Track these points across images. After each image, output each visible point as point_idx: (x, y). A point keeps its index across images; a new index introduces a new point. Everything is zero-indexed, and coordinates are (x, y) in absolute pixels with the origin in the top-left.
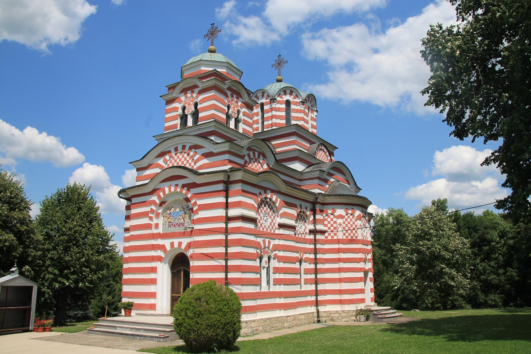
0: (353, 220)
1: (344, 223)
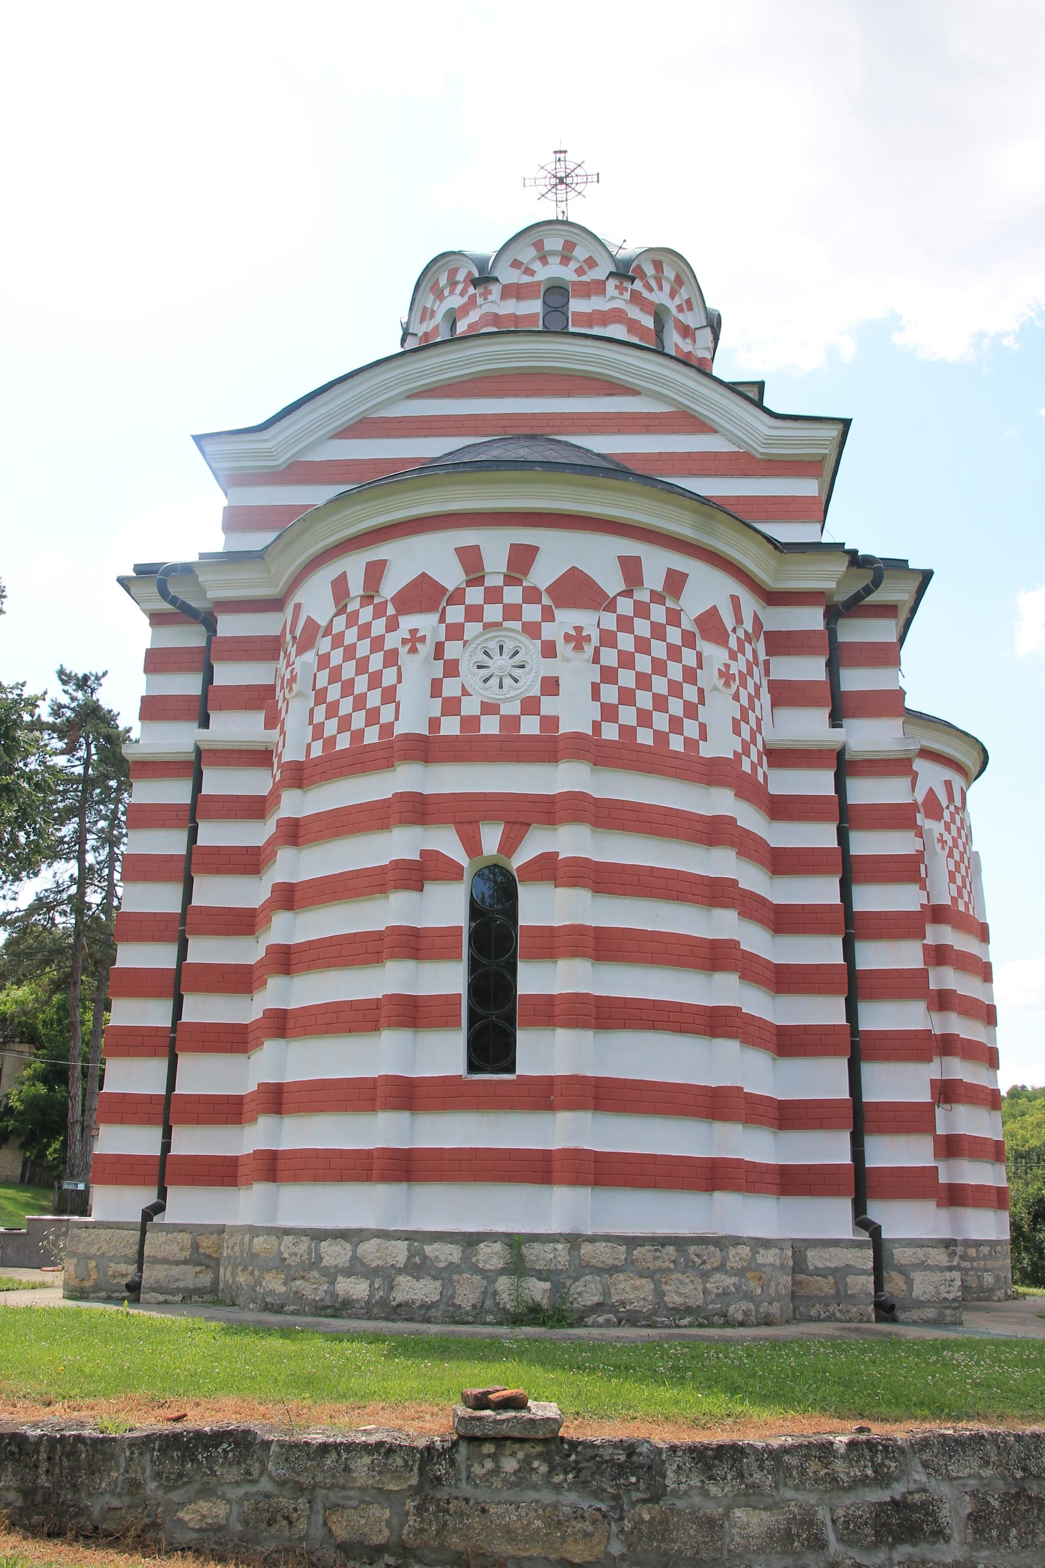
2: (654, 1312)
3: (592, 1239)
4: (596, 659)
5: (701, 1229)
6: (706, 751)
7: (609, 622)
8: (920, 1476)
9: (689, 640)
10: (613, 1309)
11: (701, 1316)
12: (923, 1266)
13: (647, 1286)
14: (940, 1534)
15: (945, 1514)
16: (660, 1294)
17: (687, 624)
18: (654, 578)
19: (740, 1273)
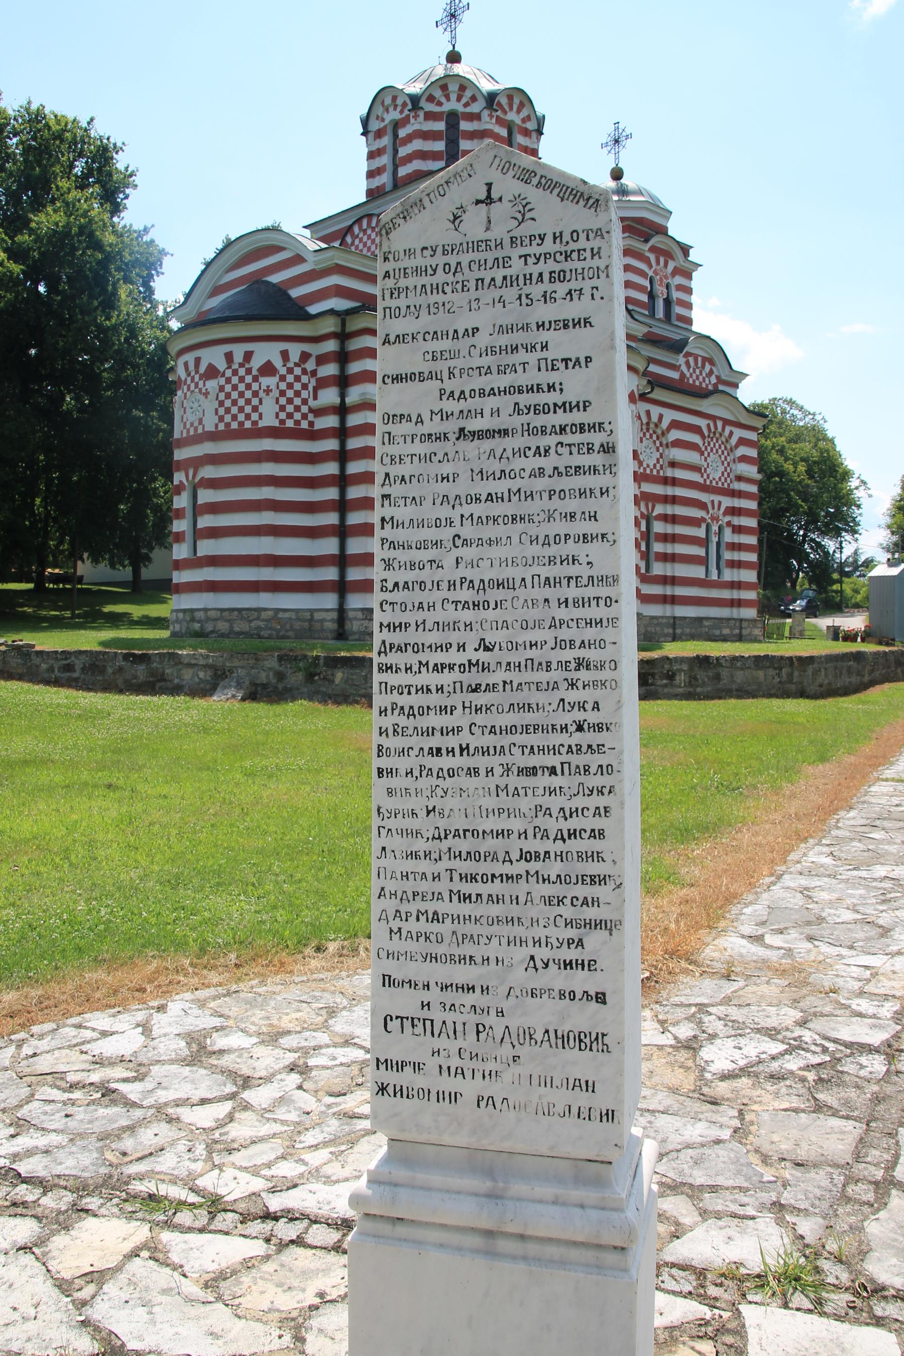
2: (229, 633)
4: (217, 398)
5: (254, 605)
6: (261, 424)
7: (222, 381)
8: (73, 658)
9: (255, 379)
10: (217, 632)
11: (248, 635)
12: (355, 619)
13: (227, 625)
14: (75, 671)
15: (76, 667)
16: (231, 627)
17: (255, 372)
18: (238, 358)
19: (268, 621)
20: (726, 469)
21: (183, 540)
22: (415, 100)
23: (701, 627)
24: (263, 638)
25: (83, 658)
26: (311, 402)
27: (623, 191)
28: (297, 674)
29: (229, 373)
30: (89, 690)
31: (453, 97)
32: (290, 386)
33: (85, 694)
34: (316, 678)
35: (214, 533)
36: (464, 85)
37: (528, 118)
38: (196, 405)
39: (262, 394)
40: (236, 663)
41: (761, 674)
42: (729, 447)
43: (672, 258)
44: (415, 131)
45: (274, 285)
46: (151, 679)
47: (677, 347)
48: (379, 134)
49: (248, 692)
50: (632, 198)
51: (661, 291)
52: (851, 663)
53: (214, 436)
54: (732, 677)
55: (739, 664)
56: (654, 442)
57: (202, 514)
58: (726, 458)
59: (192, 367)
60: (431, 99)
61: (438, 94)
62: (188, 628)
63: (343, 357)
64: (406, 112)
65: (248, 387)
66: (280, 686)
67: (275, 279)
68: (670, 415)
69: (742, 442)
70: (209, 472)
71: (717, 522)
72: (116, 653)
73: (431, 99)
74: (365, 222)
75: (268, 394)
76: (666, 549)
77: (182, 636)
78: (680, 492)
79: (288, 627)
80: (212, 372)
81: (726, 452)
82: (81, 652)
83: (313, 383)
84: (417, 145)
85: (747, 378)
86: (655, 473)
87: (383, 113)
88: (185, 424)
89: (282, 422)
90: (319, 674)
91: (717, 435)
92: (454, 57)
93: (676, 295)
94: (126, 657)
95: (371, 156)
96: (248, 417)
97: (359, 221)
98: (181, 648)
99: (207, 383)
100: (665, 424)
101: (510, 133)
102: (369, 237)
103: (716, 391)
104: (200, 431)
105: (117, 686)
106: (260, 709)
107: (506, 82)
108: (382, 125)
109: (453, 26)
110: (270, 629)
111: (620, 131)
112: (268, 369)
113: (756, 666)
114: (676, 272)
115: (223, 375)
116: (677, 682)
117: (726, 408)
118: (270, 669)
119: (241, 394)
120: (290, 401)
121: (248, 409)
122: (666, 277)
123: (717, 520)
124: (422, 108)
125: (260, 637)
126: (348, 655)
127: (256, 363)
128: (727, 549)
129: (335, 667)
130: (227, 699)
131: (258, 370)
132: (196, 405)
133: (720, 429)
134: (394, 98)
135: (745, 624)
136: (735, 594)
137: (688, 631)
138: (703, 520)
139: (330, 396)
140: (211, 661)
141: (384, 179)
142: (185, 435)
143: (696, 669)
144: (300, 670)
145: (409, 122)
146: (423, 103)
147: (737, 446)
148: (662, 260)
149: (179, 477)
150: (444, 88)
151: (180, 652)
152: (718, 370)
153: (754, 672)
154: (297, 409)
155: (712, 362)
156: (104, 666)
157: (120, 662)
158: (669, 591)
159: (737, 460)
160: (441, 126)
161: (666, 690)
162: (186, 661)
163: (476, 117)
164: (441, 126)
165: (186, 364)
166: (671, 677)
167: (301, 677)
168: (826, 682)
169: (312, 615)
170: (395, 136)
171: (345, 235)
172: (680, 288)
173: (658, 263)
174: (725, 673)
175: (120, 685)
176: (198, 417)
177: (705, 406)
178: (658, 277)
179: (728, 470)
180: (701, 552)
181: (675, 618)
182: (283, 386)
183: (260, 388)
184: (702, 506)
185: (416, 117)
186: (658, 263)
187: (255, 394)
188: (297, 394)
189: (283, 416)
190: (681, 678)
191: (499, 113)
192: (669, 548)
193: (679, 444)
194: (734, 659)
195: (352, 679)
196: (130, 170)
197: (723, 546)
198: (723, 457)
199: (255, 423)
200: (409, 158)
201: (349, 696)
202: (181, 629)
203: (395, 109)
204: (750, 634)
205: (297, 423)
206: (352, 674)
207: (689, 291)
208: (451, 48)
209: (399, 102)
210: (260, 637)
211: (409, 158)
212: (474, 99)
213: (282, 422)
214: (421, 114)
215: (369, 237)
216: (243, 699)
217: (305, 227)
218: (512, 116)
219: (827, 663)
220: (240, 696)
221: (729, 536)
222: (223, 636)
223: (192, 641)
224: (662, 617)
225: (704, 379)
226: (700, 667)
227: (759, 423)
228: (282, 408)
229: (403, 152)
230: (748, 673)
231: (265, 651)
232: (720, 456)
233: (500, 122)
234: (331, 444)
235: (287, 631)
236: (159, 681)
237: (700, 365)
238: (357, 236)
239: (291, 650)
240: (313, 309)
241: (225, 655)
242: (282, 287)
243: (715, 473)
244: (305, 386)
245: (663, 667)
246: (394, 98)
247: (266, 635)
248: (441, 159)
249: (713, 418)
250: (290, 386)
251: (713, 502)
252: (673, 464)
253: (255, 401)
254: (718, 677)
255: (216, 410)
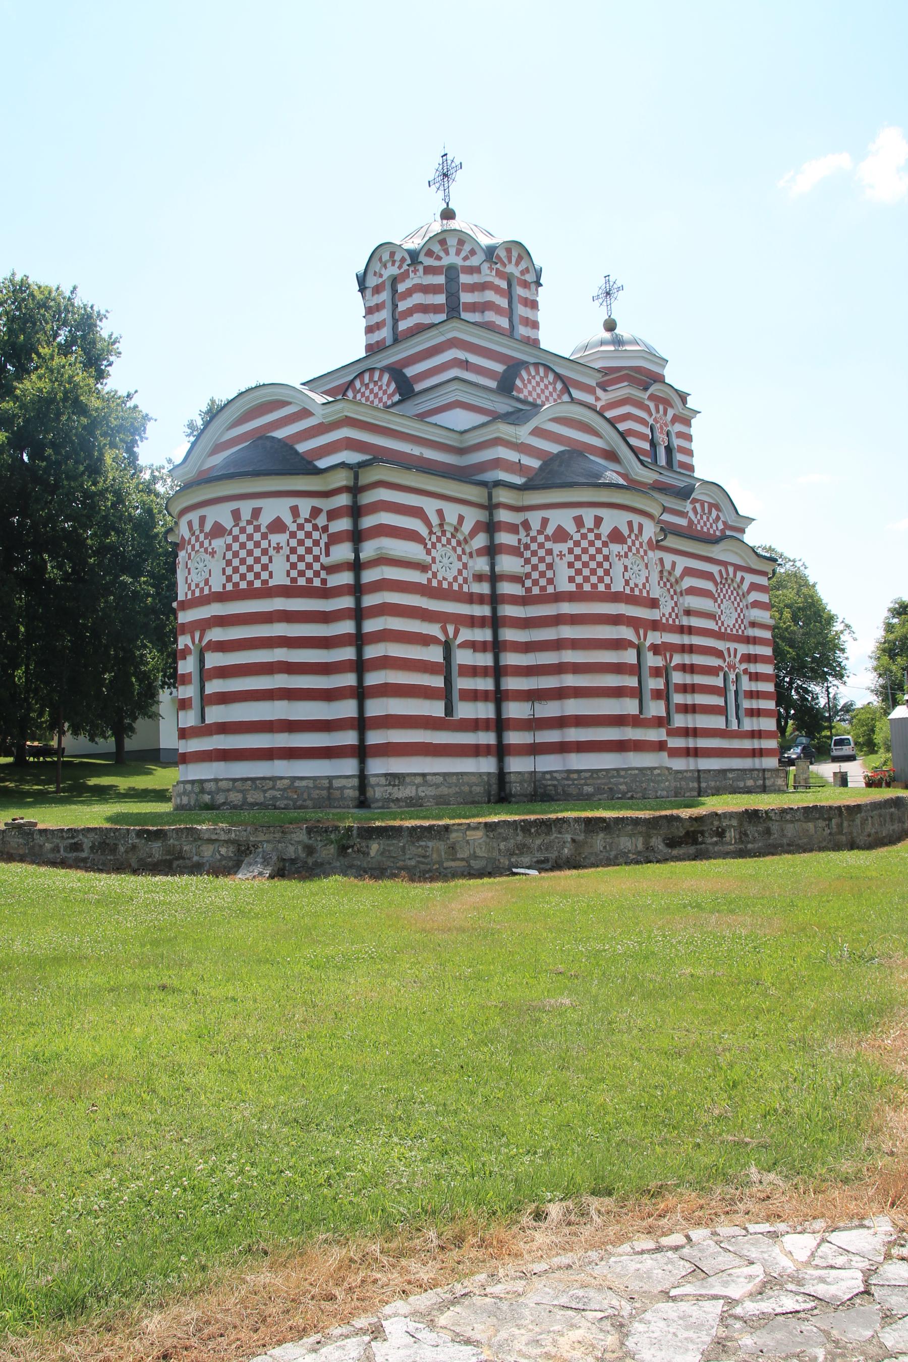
0: (598, 544)
1: (571, 551)
2: (242, 805)
3: (222, 780)
4: (224, 558)
5: (268, 774)
6: (272, 583)
7: (229, 539)
8: (81, 837)
9: (264, 536)
10: (229, 804)
11: (262, 806)
12: (378, 785)
13: (240, 796)
14: (83, 850)
15: (84, 846)
16: (245, 798)
18: (246, 515)
19: (284, 790)
20: (739, 615)
21: (190, 707)
22: (414, 255)
23: (725, 779)
24: (279, 808)
25: (91, 835)
26: (323, 559)
27: (618, 342)
28: (328, 847)
29: (236, 531)
30: (100, 871)
31: (452, 251)
32: (301, 543)
33: (97, 875)
34: (350, 850)
35: (224, 698)
36: (462, 239)
37: (527, 270)
38: (201, 565)
39: (271, 552)
40: (262, 837)
41: (811, 826)
42: (741, 593)
43: (672, 407)
44: (414, 285)
45: (280, 440)
46: (168, 857)
47: (685, 493)
48: (377, 290)
49: (276, 869)
50: (628, 348)
51: (661, 439)
52: (893, 810)
53: (221, 597)
54: (782, 830)
55: (788, 817)
56: (668, 590)
57: (210, 678)
58: (739, 605)
59: (196, 526)
60: (430, 253)
61: (437, 248)
62: (197, 800)
63: (356, 512)
64: (405, 267)
65: (257, 545)
66: (310, 861)
67: (280, 434)
68: (683, 563)
69: (754, 587)
70: (216, 634)
71: (734, 671)
72: (128, 830)
73: (430, 253)
74: (367, 377)
75: (278, 552)
76: (686, 699)
77: (190, 809)
78: (697, 640)
79: (305, 796)
80: (218, 531)
81: (738, 598)
82: (89, 830)
83: (325, 538)
84: (418, 298)
85: (754, 522)
86: (671, 622)
87: (381, 269)
88: (190, 586)
89: (294, 580)
90: (352, 847)
91: (729, 581)
92: (448, 214)
93: (677, 442)
94: (139, 834)
95: (370, 311)
96: (257, 576)
97: (360, 375)
98: (200, 822)
99: (213, 542)
100: (678, 572)
101: (510, 285)
102: (372, 391)
103: (724, 538)
104: (206, 591)
105: (130, 865)
106: (291, 888)
107: (501, 236)
108: (381, 280)
109: (446, 185)
110: (287, 798)
111: (611, 284)
112: (278, 526)
113: (805, 818)
114: (676, 419)
115: (230, 533)
116: (727, 839)
117: (736, 553)
118: (299, 842)
119: (250, 553)
120: (301, 558)
121: (257, 568)
122: (666, 426)
123: (734, 668)
124: (421, 263)
125: (276, 808)
126: (383, 825)
127: (265, 520)
128: (745, 697)
129: (370, 838)
130: (254, 877)
131: (268, 527)
132: (201, 565)
133: (731, 575)
134: (392, 254)
135: (768, 775)
136: (756, 744)
137: (713, 784)
138: (720, 668)
139: (343, 552)
140: (233, 835)
141: (385, 333)
142: (189, 597)
143: (746, 824)
144: (332, 842)
145: (408, 276)
146: (422, 258)
147: (749, 592)
148: (661, 408)
149: (184, 641)
150: (443, 242)
151: (199, 827)
152: (724, 515)
153: (804, 825)
154: (309, 566)
155: (718, 508)
156: (116, 845)
157: (133, 840)
158: (691, 743)
159: (749, 606)
160: (441, 280)
161: (716, 848)
162: (206, 836)
163: (476, 270)
164: (441, 280)
165: (190, 524)
166: (721, 834)
167: (332, 850)
168: (873, 831)
169: (330, 783)
170: (394, 291)
171: (347, 390)
172: (680, 435)
173: (658, 411)
174: (775, 827)
175: (133, 864)
176: (204, 578)
177: (716, 552)
178: (658, 425)
179: (742, 617)
180: (720, 701)
181: (699, 771)
182: (293, 543)
183: (270, 546)
184: (719, 654)
185: (415, 271)
186: (658, 411)
187: (265, 552)
188: (309, 551)
189: (294, 574)
190: (731, 835)
191: (498, 266)
192: (689, 699)
193: (693, 591)
194: (784, 811)
195: (389, 851)
196: (114, 337)
197: (741, 695)
198: (736, 603)
199: (265, 582)
200: (409, 312)
201: (386, 869)
202: (189, 802)
203: (393, 264)
204: (773, 785)
205: (310, 580)
206: (389, 845)
207: (689, 438)
208: (445, 206)
209: (397, 257)
210: (275, 808)
211: (409, 312)
212: (473, 252)
213: (294, 580)
214: (421, 268)
215: (372, 391)
216: (272, 877)
217: (303, 384)
218: (511, 269)
219: (872, 811)
220: (267, 872)
221: (746, 685)
222: (235, 807)
223: (206, 814)
224: (686, 771)
225: (711, 525)
226: (750, 822)
227: (767, 567)
228: (294, 566)
229: (403, 306)
230: (797, 825)
231: (291, 823)
232: (733, 603)
233: (500, 274)
234: (347, 602)
235: (305, 800)
236: (177, 859)
237: (706, 511)
238: (359, 391)
239: (318, 821)
240: (322, 464)
241: (249, 829)
242: (289, 442)
243: (729, 620)
244: (316, 543)
245: (712, 823)
246: (392, 254)
247: (283, 806)
248: (442, 312)
249: (725, 564)
250: (301, 543)
251: (728, 649)
252: (688, 613)
253: (265, 559)
254: (768, 832)
255: (224, 570)
